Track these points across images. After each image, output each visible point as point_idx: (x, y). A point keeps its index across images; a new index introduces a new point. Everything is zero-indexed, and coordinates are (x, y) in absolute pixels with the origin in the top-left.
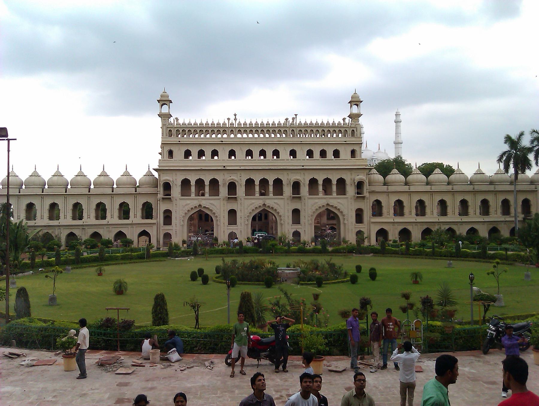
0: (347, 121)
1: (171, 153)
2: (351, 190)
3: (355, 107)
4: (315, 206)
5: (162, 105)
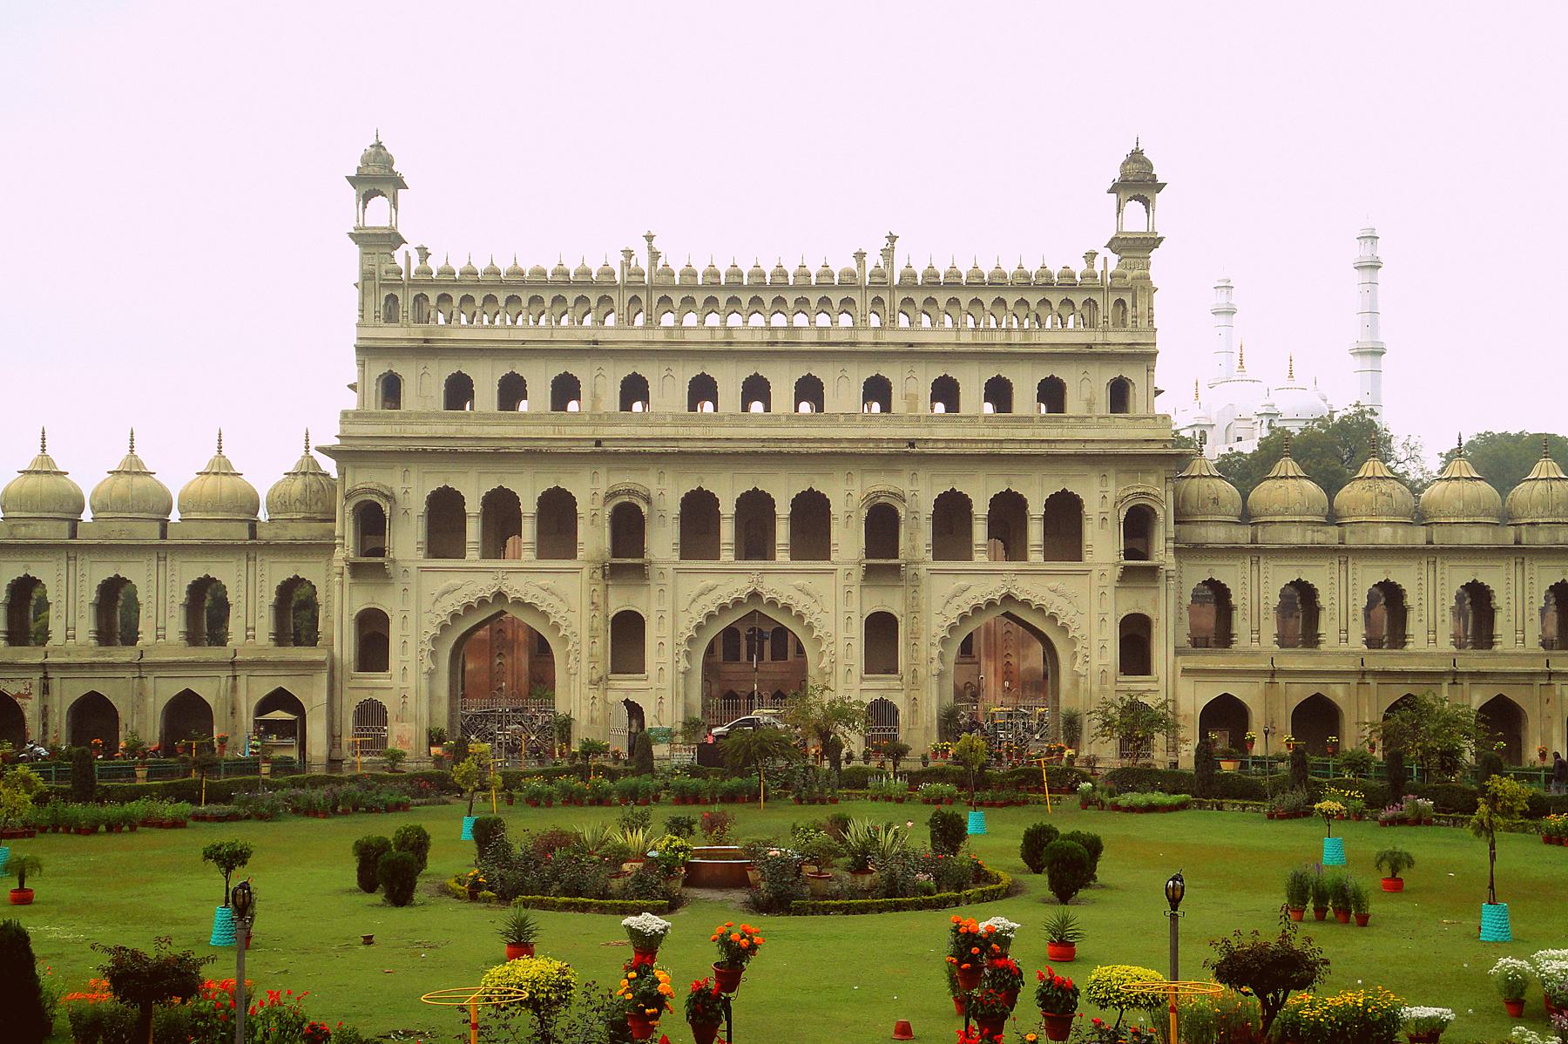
0: (1098, 267)
1: (391, 389)
2: (1103, 542)
3: (1134, 208)
4: (956, 601)
5: (366, 198)
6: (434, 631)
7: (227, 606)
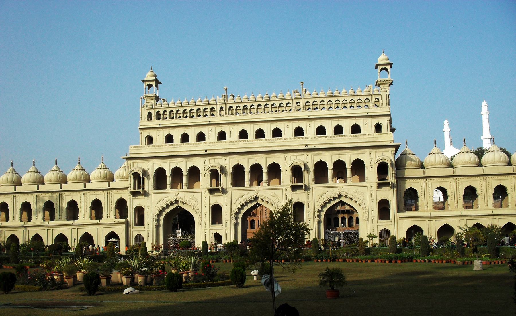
6: (157, 212)
7: (102, 208)
